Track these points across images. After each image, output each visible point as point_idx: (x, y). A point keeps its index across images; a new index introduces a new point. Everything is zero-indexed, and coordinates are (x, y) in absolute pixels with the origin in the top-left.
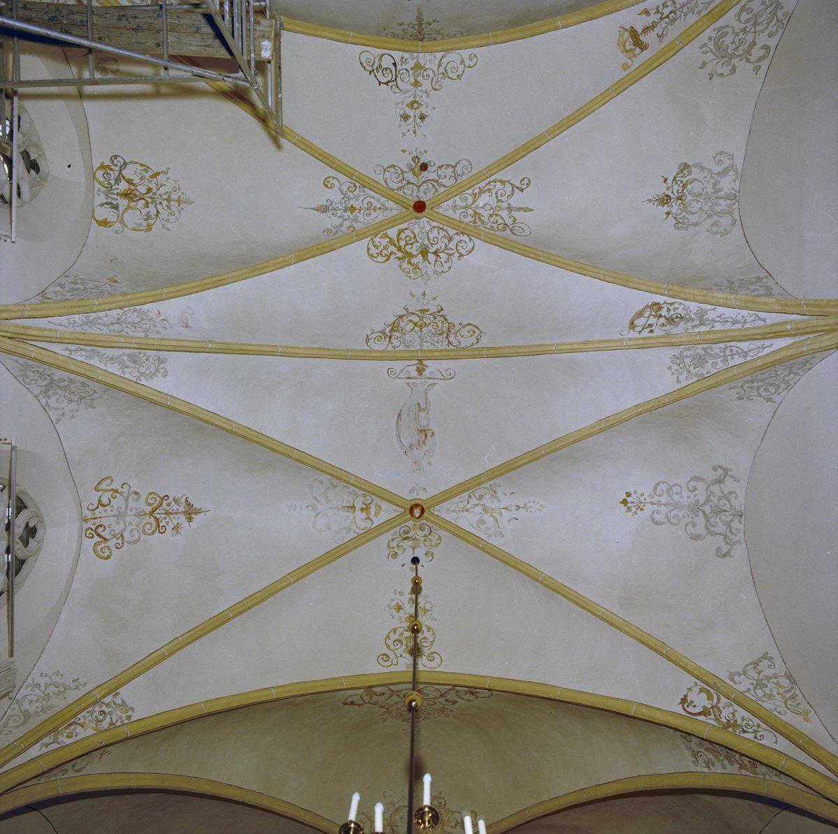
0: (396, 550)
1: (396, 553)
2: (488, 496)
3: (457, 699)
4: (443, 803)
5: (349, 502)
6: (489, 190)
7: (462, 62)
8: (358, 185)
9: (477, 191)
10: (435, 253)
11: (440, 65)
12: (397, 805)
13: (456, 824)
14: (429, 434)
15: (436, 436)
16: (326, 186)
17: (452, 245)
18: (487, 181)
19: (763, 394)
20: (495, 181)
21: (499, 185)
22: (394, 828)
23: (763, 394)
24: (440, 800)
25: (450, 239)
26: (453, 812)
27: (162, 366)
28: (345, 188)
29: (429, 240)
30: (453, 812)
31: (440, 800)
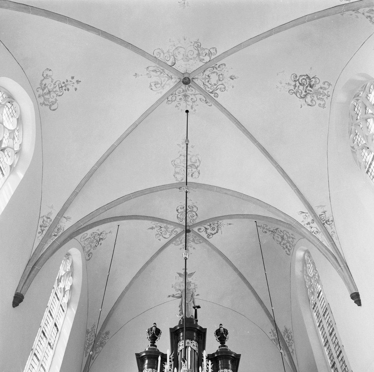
4: (200, 45)
12: (177, 46)
13: (206, 55)
22: (175, 57)
24: (198, 44)
26: (204, 49)
30: (204, 49)
31: (198, 44)
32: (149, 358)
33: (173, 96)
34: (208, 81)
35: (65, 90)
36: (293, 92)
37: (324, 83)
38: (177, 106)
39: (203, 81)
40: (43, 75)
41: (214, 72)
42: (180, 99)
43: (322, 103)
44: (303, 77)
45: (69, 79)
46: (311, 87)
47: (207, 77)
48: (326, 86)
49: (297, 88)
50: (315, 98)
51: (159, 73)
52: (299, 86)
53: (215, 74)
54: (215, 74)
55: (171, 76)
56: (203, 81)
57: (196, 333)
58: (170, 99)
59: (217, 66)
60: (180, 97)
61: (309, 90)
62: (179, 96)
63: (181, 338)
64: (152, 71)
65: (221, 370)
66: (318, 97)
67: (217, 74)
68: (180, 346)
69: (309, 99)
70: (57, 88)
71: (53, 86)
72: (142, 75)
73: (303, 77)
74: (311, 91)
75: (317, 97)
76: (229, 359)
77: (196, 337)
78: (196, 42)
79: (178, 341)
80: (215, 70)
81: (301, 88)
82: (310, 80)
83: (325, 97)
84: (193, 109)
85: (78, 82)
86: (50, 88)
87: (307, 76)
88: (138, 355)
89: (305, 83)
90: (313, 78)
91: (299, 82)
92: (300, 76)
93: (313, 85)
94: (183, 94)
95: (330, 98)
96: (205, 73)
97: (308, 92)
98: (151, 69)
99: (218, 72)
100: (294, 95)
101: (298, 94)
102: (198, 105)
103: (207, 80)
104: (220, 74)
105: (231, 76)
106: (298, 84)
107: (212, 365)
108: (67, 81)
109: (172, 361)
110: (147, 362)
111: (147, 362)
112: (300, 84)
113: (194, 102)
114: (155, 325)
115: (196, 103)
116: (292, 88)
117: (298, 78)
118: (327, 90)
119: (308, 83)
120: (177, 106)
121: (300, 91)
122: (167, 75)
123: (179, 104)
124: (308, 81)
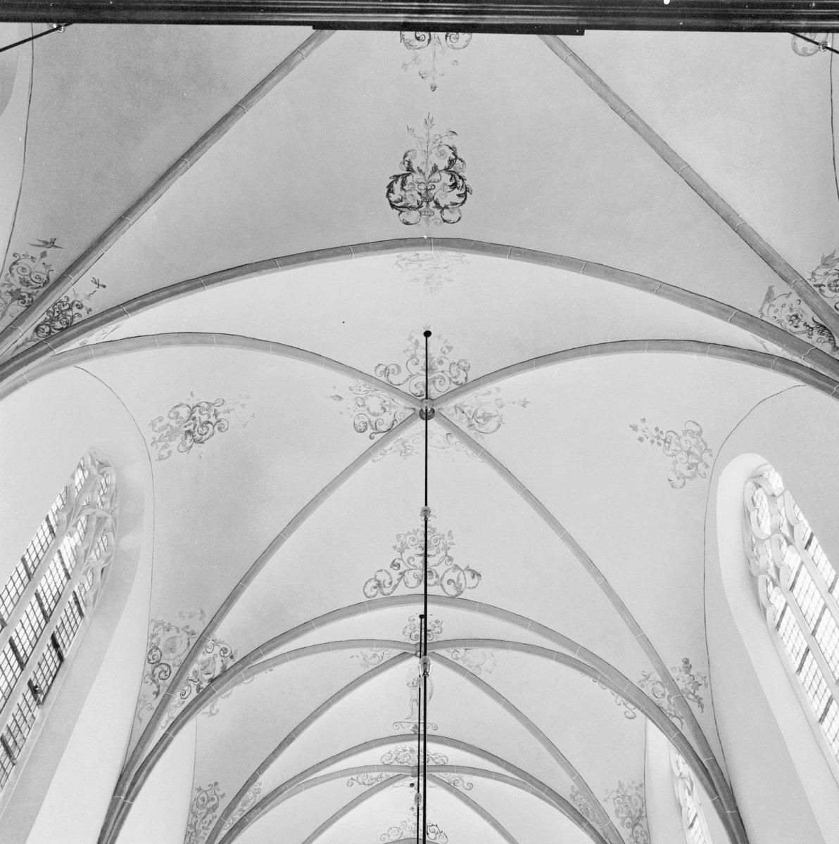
0: (436, 625)
1: (436, 623)
2: (369, 656)
3: (391, 570)
5: (469, 653)
6: (372, 779)
7: (389, 836)
8: (452, 784)
9: (380, 780)
10: (405, 751)
11: (402, 833)
14: (411, 684)
15: (406, 683)
16: (472, 784)
17: (394, 756)
18: (374, 785)
19: (204, 795)
20: (369, 785)
21: (367, 783)
23: (204, 795)
25: (396, 759)
27: (574, 794)
28: (461, 782)
29: (410, 756)
33: (455, 377)
34: (385, 401)
35: (662, 432)
36: (217, 404)
37: (169, 453)
38: (450, 348)
39: (393, 403)
40: (684, 484)
41: (374, 414)
42: (441, 362)
43: (159, 425)
44: (207, 436)
45: (647, 441)
46: (189, 432)
47: (387, 409)
48: (164, 453)
49: (212, 413)
50: (173, 423)
51: (479, 414)
52: (210, 418)
53: (372, 411)
54: (372, 411)
55: (456, 411)
56: (393, 403)
58: (463, 374)
59: (369, 431)
60: (440, 368)
61: (190, 425)
62: (443, 372)
64: (492, 417)
66: (169, 428)
67: (368, 409)
69: (184, 412)
70: (673, 446)
71: (679, 456)
72: (514, 403)
73: (207, 436)
74: (185, 427)
75: (171, 427)
78: (408, 455)
80: (373, 419)
81: (204, 418)
82: (194, 441)
83: (157, 436)
84: (414, 341)
85: (635, 428)
86: (683, 456)
87: (202, 443)
89: (200, 429)
90: (191, 447)
91: (211, 423)
92: (213, 434)
93: (186, 438)
94: (436, 375)
95: (149, 441)
96: (391, 419)
97: (191, 421)
98: (492, 424)
99: (366, 412)
100: (212, 401)
101: (206, 406)
102: (404, 352)
103: (387, 403)
104: (362, 408)
105: (340, 400)
106: (213, 420)
108: (652, 442)
112: (209, 422)
113: (413, 357)
115: (409, 354)
116: (219, 409)
117: (216, 427)
118: (160, 447)
119: (196, 433)
120: (450, 348)
121: (204, 412)
122: (463, 412)
123: (444, 352)
124: (198, 436)
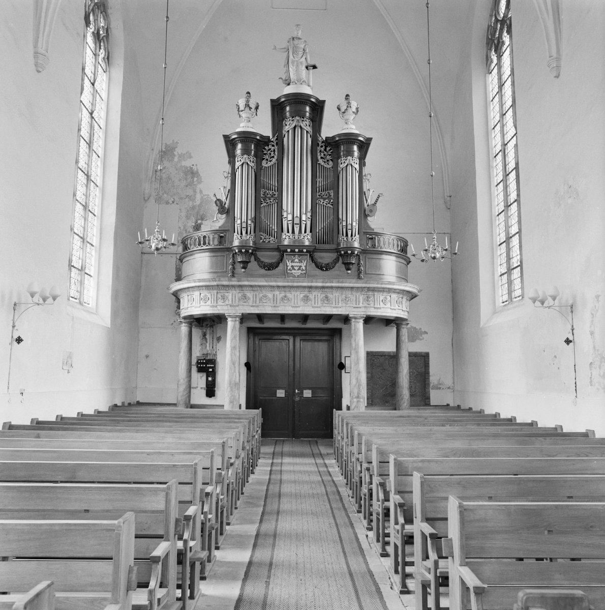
32: (242, 142)
57: (310, 107)
63: (288, 114)
65: (343, 158)
68: (286, 125)
76: (354, 143)
77: (310, 114)
79: (283, 118)
88: (226, 138)
107: (331, 151)
109: (275, 146)
110: (239, 146)
111: (239, 146)
114: (249, 95)
